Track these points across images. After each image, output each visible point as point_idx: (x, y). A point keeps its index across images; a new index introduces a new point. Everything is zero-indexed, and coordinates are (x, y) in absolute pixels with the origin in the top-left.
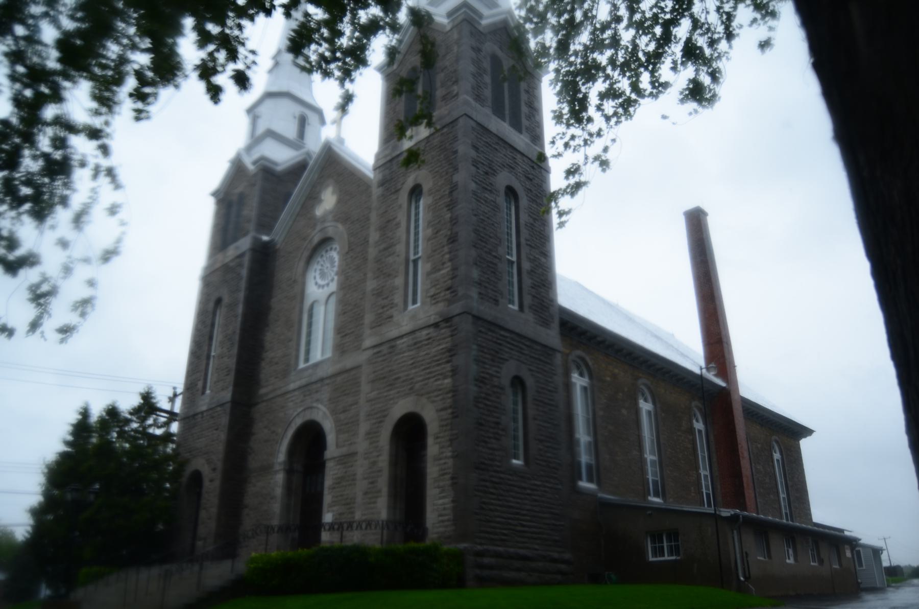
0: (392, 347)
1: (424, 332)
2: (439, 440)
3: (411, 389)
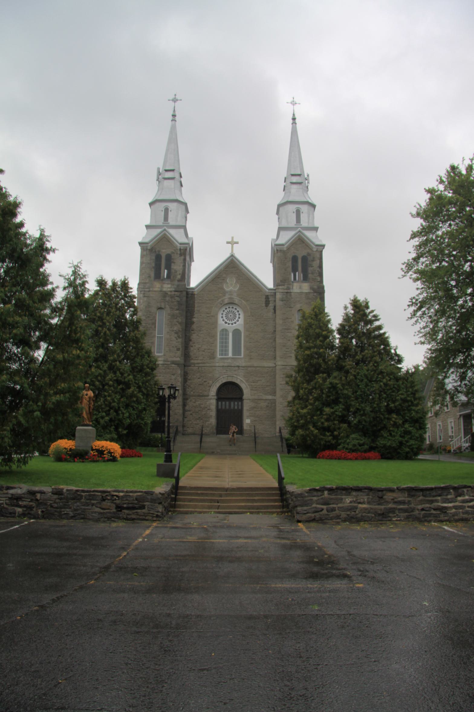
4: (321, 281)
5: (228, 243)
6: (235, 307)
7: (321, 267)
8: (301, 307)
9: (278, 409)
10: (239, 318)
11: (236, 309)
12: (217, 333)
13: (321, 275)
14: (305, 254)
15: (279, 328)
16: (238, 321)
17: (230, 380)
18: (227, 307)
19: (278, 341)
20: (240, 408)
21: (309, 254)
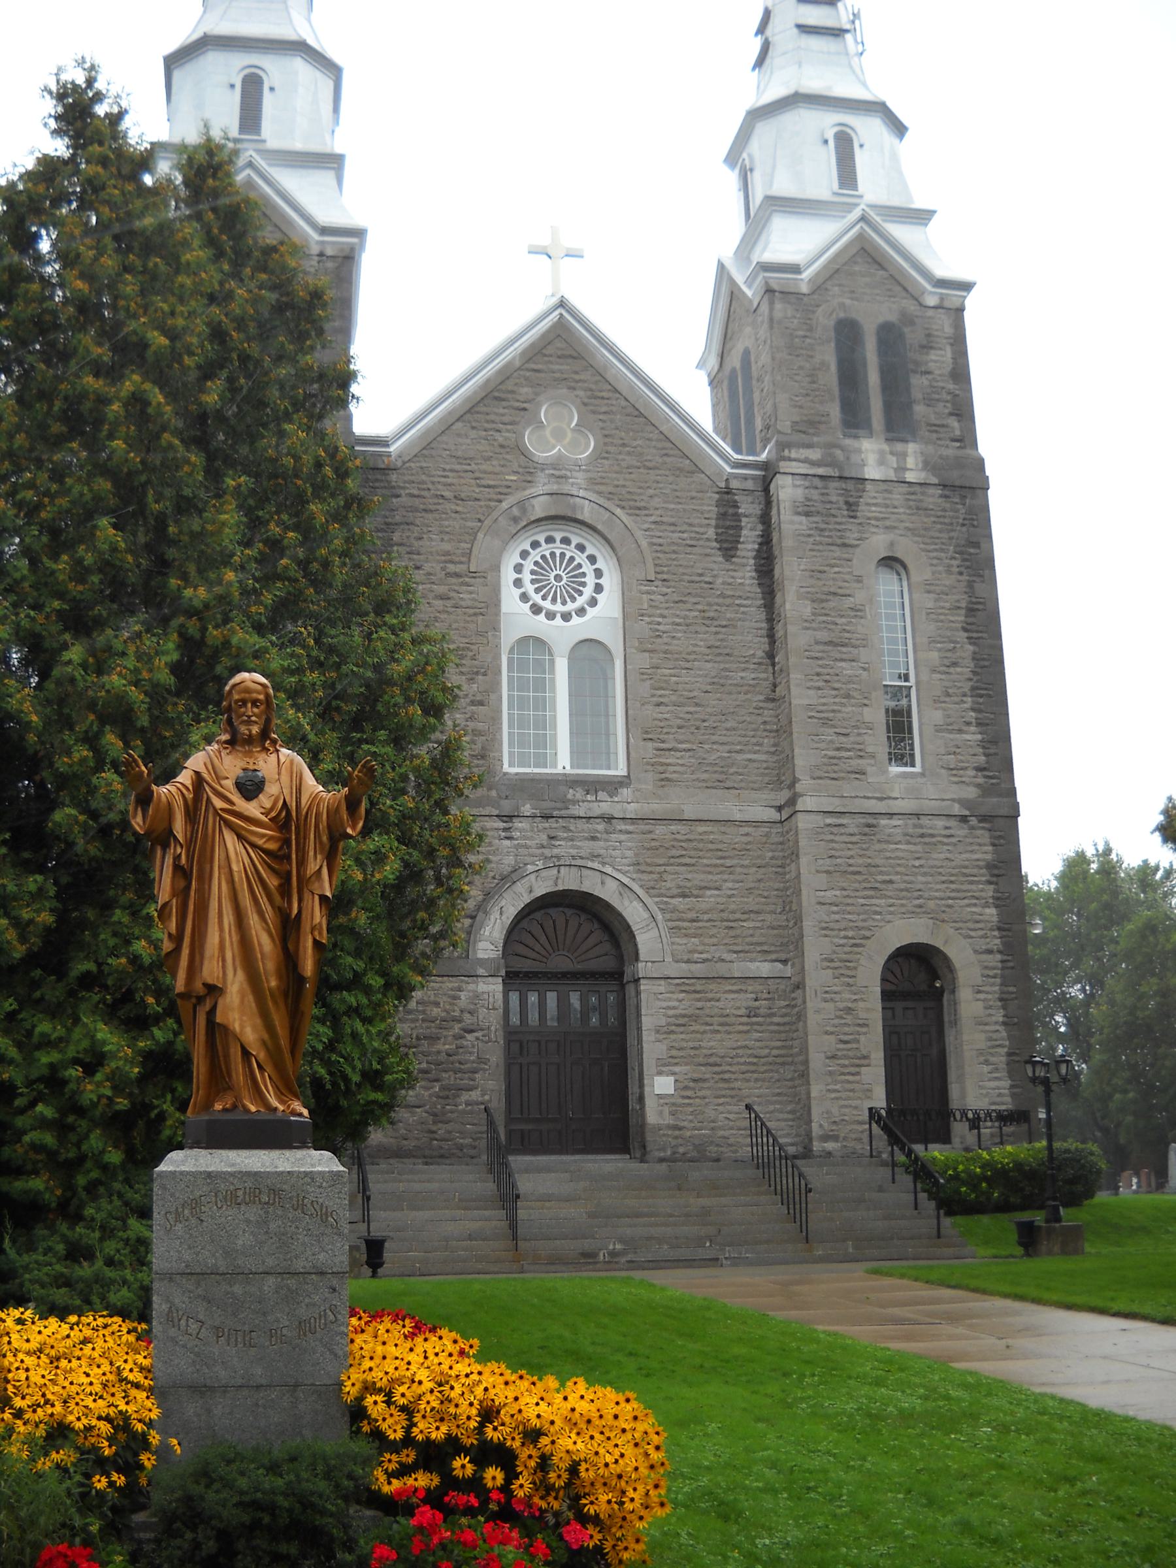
0: (869, 826)
1: (940, 823)
2: (982, 996)
3: (920, 906)
4: (968, 438)
5: (533, 251)
6: (575, 540)
7: (960, 374)
8: (892, 544)
9: (812, 1019)
10: (599, 588)
11: (581, 548)
12: (498, 657)
13: (963, 410)
14: (893, 318)
15: (797, 637)
16: (593, 602)
17: (569, 881)
18: (541, 538)
19: (801, 696)
20: (612, 1020)
21: (908, 319)
